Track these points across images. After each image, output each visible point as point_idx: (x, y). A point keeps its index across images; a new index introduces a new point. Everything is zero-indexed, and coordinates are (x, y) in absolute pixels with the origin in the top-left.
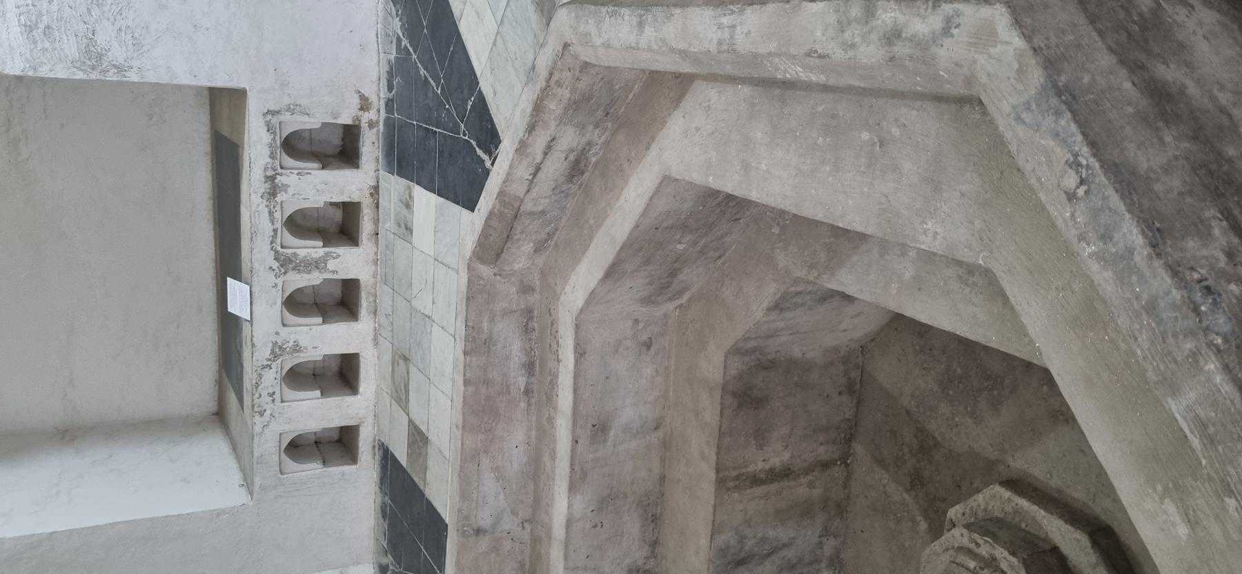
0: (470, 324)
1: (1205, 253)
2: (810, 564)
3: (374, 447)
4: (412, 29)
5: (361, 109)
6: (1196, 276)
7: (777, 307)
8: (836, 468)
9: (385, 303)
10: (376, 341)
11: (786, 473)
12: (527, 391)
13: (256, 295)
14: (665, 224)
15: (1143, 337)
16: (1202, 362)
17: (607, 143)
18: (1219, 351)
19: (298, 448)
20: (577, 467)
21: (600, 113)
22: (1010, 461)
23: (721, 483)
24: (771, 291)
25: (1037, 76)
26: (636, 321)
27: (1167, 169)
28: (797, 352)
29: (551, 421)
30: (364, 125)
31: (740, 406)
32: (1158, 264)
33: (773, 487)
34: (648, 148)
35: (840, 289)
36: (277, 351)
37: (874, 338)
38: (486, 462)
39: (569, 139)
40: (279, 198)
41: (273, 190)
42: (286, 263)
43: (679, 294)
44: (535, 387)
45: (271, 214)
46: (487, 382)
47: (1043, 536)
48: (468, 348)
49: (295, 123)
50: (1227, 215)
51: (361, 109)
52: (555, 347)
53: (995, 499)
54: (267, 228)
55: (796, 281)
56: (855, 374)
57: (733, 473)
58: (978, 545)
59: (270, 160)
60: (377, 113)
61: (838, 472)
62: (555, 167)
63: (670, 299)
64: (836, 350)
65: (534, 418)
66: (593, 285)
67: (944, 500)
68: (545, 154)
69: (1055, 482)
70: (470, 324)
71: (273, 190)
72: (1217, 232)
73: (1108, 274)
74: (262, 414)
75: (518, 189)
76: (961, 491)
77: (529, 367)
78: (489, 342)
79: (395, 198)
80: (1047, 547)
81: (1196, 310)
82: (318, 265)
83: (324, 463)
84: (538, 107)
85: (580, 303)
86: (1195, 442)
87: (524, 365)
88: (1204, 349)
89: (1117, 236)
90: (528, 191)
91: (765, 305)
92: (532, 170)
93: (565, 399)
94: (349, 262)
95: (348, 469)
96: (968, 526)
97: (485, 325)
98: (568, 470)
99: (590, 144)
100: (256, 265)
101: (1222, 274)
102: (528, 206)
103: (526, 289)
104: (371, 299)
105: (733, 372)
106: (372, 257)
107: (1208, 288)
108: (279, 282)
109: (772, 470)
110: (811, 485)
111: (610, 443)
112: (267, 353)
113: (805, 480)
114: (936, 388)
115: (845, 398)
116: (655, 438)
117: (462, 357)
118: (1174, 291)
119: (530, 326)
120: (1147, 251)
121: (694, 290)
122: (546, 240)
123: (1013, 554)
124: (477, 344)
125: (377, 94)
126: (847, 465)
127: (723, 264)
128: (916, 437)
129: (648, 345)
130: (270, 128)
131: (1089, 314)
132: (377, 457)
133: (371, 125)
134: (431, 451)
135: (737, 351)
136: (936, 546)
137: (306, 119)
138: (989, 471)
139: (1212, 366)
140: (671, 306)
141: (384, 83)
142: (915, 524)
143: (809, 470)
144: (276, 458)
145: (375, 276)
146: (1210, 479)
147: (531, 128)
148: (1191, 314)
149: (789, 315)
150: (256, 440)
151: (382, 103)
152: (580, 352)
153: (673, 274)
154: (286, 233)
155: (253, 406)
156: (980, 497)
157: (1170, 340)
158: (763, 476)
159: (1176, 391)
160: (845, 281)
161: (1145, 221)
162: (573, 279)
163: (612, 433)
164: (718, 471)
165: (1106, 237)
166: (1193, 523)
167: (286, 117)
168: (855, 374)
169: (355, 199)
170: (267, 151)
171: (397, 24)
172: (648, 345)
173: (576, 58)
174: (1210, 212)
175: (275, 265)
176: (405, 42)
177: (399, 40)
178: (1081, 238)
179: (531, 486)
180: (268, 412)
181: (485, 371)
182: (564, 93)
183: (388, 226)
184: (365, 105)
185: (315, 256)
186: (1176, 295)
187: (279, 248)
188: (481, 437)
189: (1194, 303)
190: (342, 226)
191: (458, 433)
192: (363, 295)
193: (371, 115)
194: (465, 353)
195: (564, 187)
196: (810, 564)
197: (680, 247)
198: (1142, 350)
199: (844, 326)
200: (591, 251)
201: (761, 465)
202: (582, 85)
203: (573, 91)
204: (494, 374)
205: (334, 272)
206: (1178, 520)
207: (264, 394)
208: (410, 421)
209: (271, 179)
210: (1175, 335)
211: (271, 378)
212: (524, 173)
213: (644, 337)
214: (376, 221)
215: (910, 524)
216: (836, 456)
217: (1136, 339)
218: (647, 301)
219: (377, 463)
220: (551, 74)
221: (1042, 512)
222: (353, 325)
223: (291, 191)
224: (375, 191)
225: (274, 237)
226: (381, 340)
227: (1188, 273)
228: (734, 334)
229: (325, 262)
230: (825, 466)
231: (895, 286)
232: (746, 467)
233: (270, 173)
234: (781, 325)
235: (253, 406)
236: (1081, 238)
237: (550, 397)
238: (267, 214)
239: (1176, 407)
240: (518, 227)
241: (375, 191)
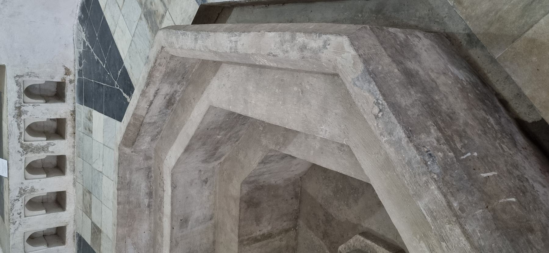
0: (120, 175)
1: (429, 140)
3: (74, 236)
4: (91, 37)
5: (66, 74)
6: (426, 150)
7: (263, 162)
8: (291, 232)
9: (79, 167)
10: (74, 184)
11: (269, 236)
12: (149, 206)
13: (11, 165)
14: (211, 127)
15: (407, 176)
16: (430, 186)
17: (184, 91)
18: (435, 180)
19: (34, 239)
20: (174, 240)
21: (180, 78)
22: (363, 224)
23: (241, 242)
24: (260, 155)
25: (361, 67)
26: (200, 171)
27: (413, 105)
28: (273, 181)
29: (160, 219)
30: (67, 82)
31: (248, 207)
32: (411, 145)
33: (265, 242)
34: (202, 93)
35: (289, 154)
36: (22, 192)
37: (305, 173)
38: (129, 241)
39: (166, 89)
40: (23, 117)
41: (19, 113)
42: (26, 149)
43: (219, 158)
44: (153, 204)
45: (18, 125)
46: (129, 203)
48: (119, 187)
49: (30, 81)
50: (436, 124)
51: (66, 74)
52: (162, 184)
54: (16, 132)
55: (271, 151)
56: (298, 189)
57: (246, 238)
59: (18, 99)
60: (74, 76)
61: (292, 233)
62: (159, 102)
63: (215, 160)
64: (289, 179)
65: (153, 218)
66: (179, 155)
68: (155, 96)
69: (381, 232)
70: (120, 175)
71: (19, 113)
72: (432, 131)
73: (392, 149)
74: (14, 223)
75: (142, 112)
76: (343, 239)
77: (150, 194)
78: (130, 183)
79: (83, 116)
81: (426, 164)
82: (44, 149)
83: (48, 246)
84: (150, 75)
85: (173, 164)
86: (429, 219)
87: (147, 194)
88: (430, 180)
89: (395, 133)
90: (147, 113)
91: (257, 161)
92: (148, 103)
93: (167, 208)
94: (60, 147)
95: (61, 248)
97: (128, 176)
98: (169, 242)
99: (176, 92)
100: (11, 151)
101: (435, 149)
102: (147, 120)
103: (148, 158)
104: (72, 164)
105: (245, 192)
106: (72, 144)
107: (430, 154)
108: (23, 158)
109: (263, 235)
110: (281, 240)
111: (189, 227)
112: (17, 193)
113: (278, 238)
114: (332, 194)
115: (294, 200)
116: (210, 224)
117: (116, 191)
118: (418, 156)
119: (150, 175)
120: (407, 139)
121: (226, 156)
122: (157, 135)
124: (123, 185)
125: (74, 68)
126: (296, 230)
127: (239, 144)
128: (324, 215)
129: (206, 182)
130: (17, 84)
131: (387, 165)
132: (76, 241)
133: (71, 82)
134: (103, 236)
135: (246, 182)
137: (37, 79)
138: (355, 229)
139: (433, 187)
140: (216, 163)
141: (77, 63)
143: (280, 233)
144: (22, 245)
145: (74, 153)
146: (435, 235)
147: (147, 85)
148: (424, 166)
149: (268, 165)
150: (11, 237)
151: (77, 72)
152: (174, 187)
153: (216, 149)
154: (27, 134)
155: (9, 220)
156: (351, 241)
157: (417, 176)
158: (259, 238)
159: (420, 197)
160: (291, 150)
161: (405, 127)
162: (170, 153)
163: (190, 223)
164: (239, 237)
165: (390, 134)
167: (26, 78)
168: (298, 189)
169: (63, 116)
170: (16, 95)
171: (83, 35)
172: (206, 182)
173: (168, 53)
174: (430, 123)
175: (21, 150)
176: (87, 43)
177: (84, 43)
178: (381, 134)
179: (152, 250)
180: (17, 223)
181: (128, 197)
182: (163, 69)
183: (80, 129)
184: (68, 72)
185: (42, 145)
186: (418, 157)
187: (23, 142)
188: (127, 229)
189: (425, 161)
190: (57, 130)
191: (115, 228)
192: (68, 162)
193: (71, 77)
194: (118, 190)
195: (164, 111)
197: (219, 137)
198: (407, 181)
199: (292, 169)
200: (177, 141)
201: (258, 233)
202: (172, 65)
203: (167, 67)
204: (132, 199)
205: (52, 152)
206: (426, 250)
207: (15, 214)
208: (92, 223)
209: (19, 108)
210: (419, 174)
211: (19, 206)
212: (144, 105)
213: (204, 178)
214: (74, 127)
216: (291, 226)
217: (404, 176)
218: (205, 161)
219: (75, 244)
220: (156, 60)
221: (376, 246)
222: (63, 177)
223: (29, 114)
224: (73, 113)
225: (20, 136)
226: (77, 184)
227: (422, 148)
228: (244, 175)
229: (48, 148)
230: (287, 231)
231: (312, 152)
232: (252, 234)
233: (17, 105)
234: (265, 170)
235: (9, 220)
236: (381, 134)
237: (160, 208)
238: (16, 125)
239: (421, 205)
240: (143, 130)
241: (73, 113)
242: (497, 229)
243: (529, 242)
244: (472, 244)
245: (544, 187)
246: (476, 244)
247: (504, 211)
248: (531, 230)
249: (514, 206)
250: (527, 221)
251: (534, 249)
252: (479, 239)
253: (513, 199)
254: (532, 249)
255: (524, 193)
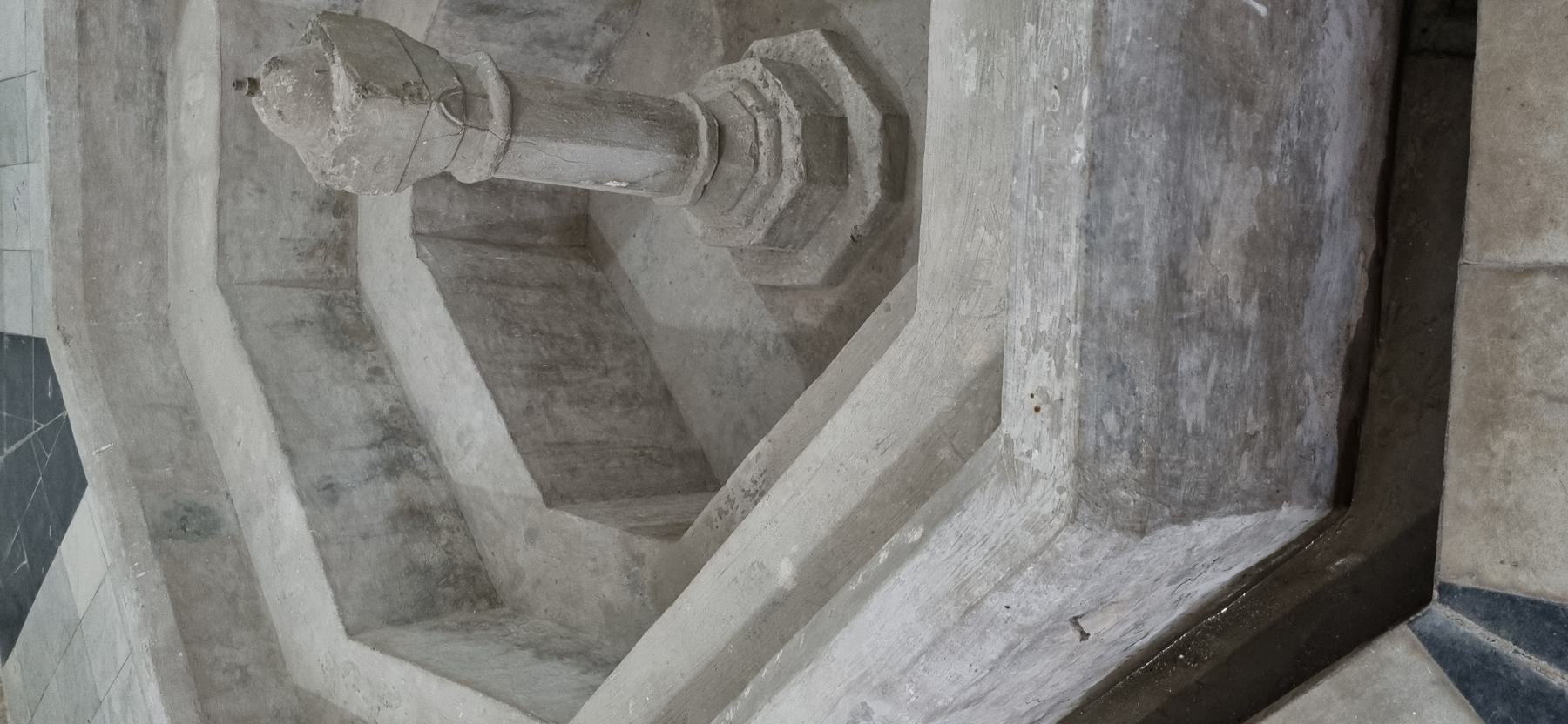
2: (573, 48)
22: (845, 12)
47: (837, 102)
53: (808, 45)
58: (766, 85)
67: (754, 30)
69: (878, 52)
76: (777, 25)
80: (836, 114)
96: (764, 61)
123: (798, 107)
136: (722, 71)
142: (711, 46)
156: (794, 39)
166: (984, 80)
196: (573, 48)
215: (705, 45)
221: (850, 77)
242: (1179, 48)
243: (1225, 120)
244: (1097, 48)
245: (1349, 33)
246: (1107, 55)
247: (1222, 20)
248: (1248, 100)
249: (1251, 25)
250: (1256, 75)
251: (1223, 142)
252: (1122, 48)
253: (1262, 10)
254: (1219, 137)
255: (1295, 13)
